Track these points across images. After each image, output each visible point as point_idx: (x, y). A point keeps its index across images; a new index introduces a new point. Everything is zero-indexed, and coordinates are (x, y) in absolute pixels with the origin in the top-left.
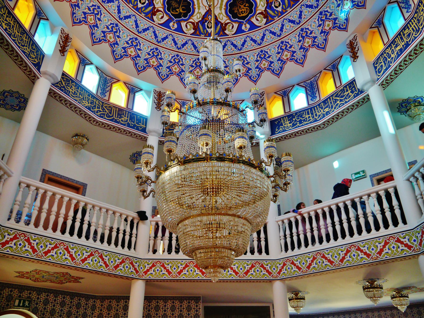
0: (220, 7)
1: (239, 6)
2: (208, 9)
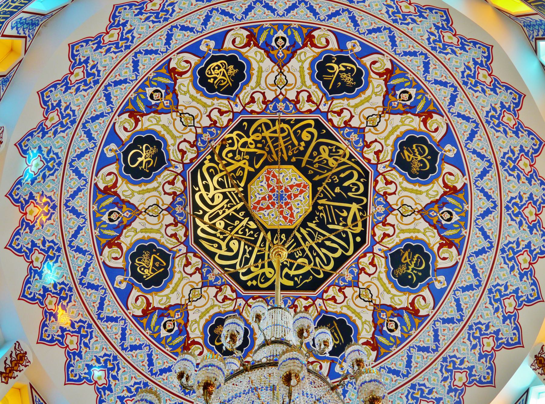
0: (262, 72)
1: (225, 77)
2: (285, 68)
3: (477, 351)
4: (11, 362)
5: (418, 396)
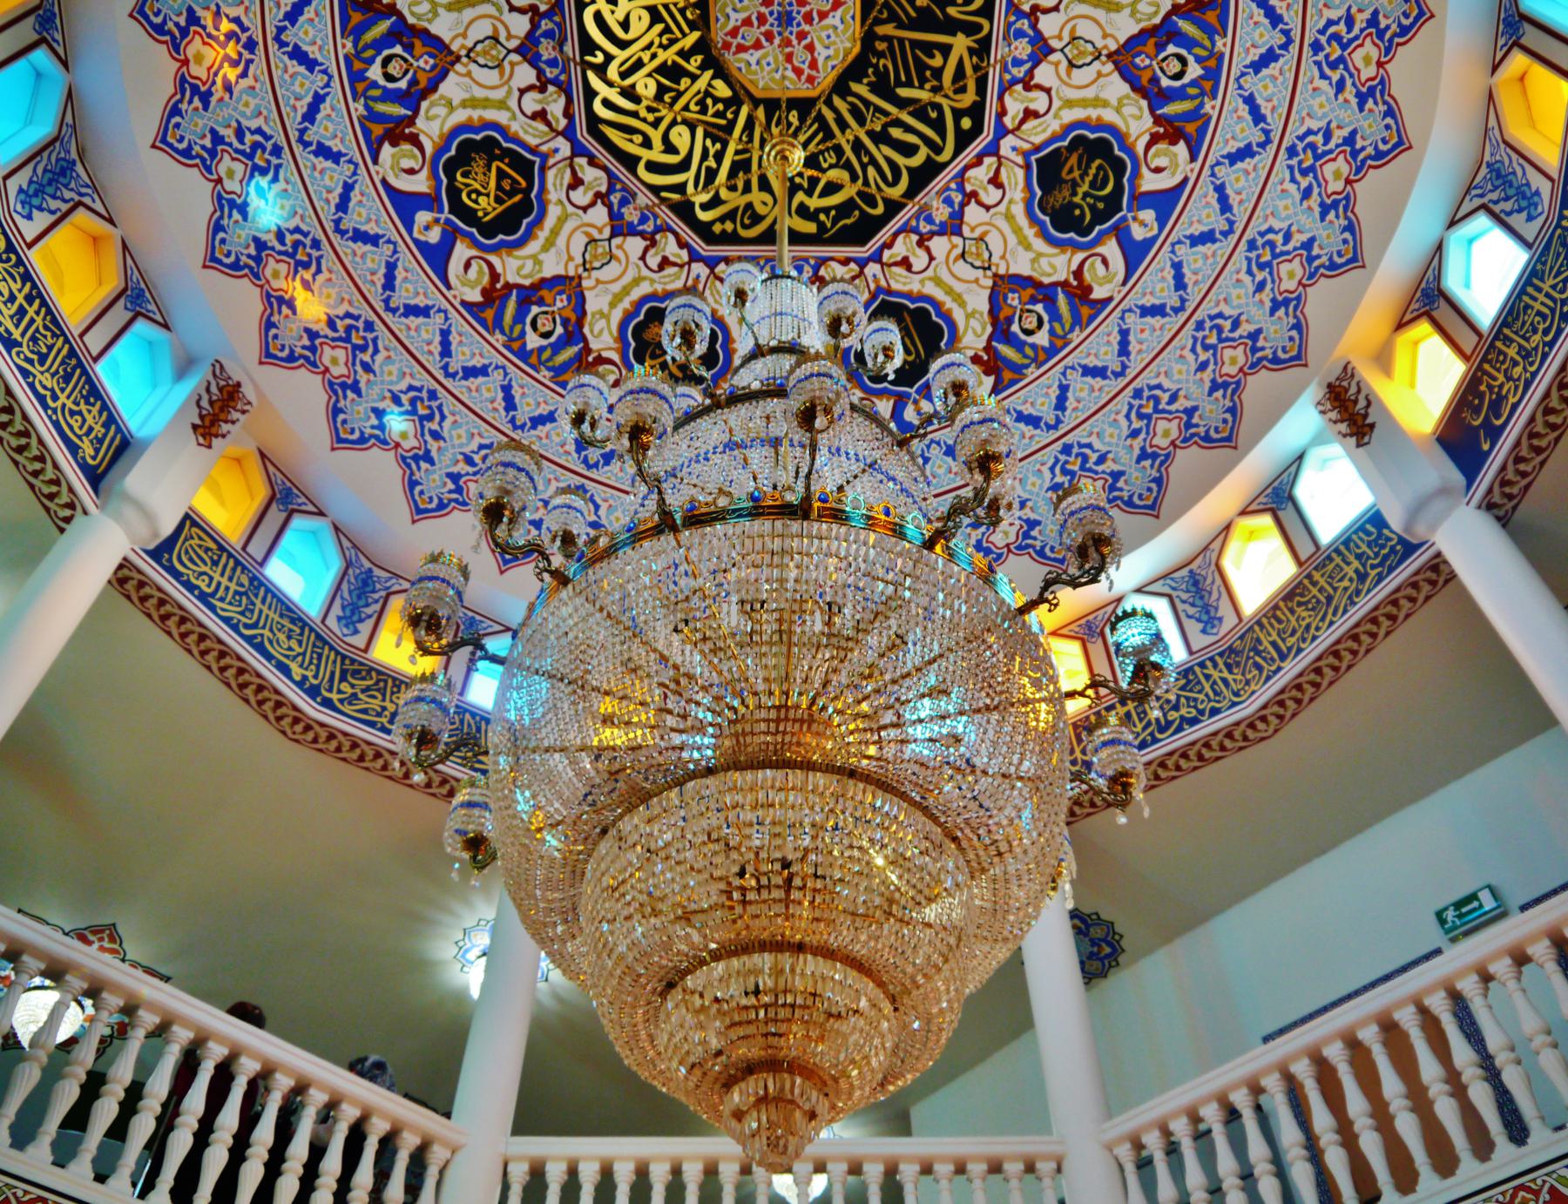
3: (1207, 375)
4: (211, 403)
5: (1076, 468)
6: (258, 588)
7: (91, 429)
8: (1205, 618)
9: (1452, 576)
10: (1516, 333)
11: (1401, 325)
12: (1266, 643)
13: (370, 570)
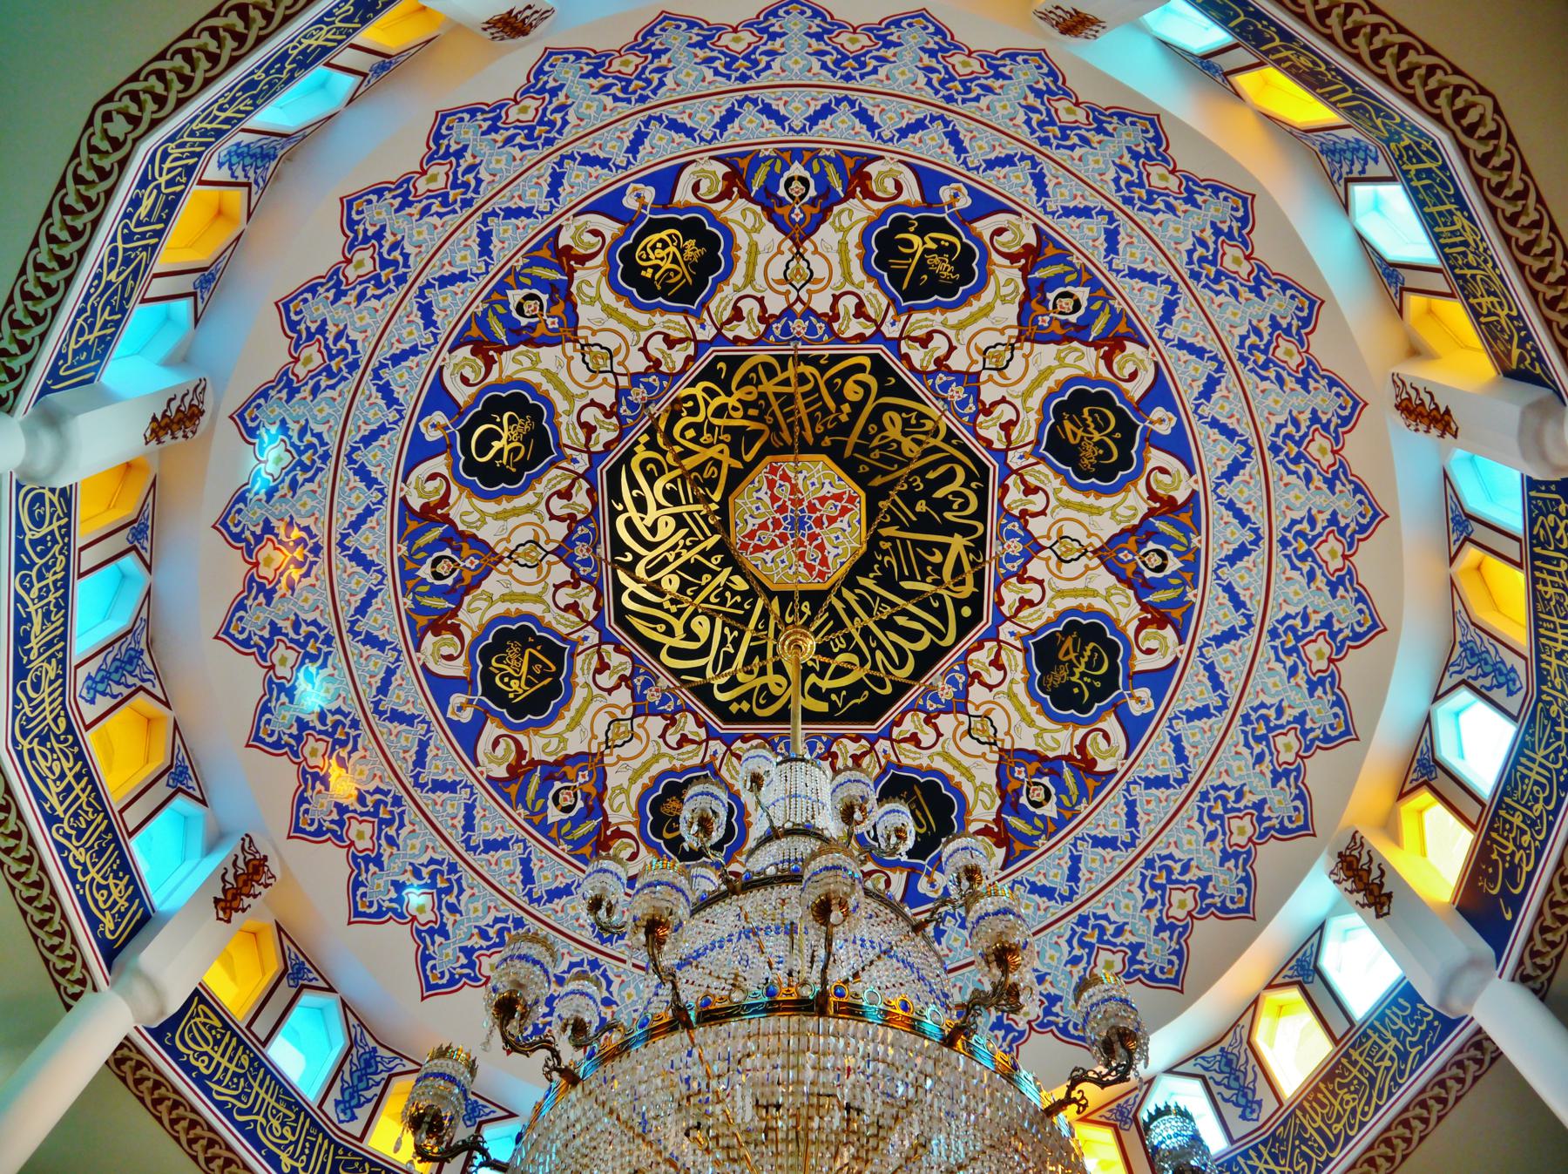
2: (807, 244)
3: (1217, 845)
4: (236, 877)
5: (1094, 940)
6: (257, 1070)
7: (115, 903)
8: (1242, 1101)
9: (1498, 1054)
10: (1517, 802)
11: (1402, 795)
12: (1310, 1130)
13: (374, 1050)
